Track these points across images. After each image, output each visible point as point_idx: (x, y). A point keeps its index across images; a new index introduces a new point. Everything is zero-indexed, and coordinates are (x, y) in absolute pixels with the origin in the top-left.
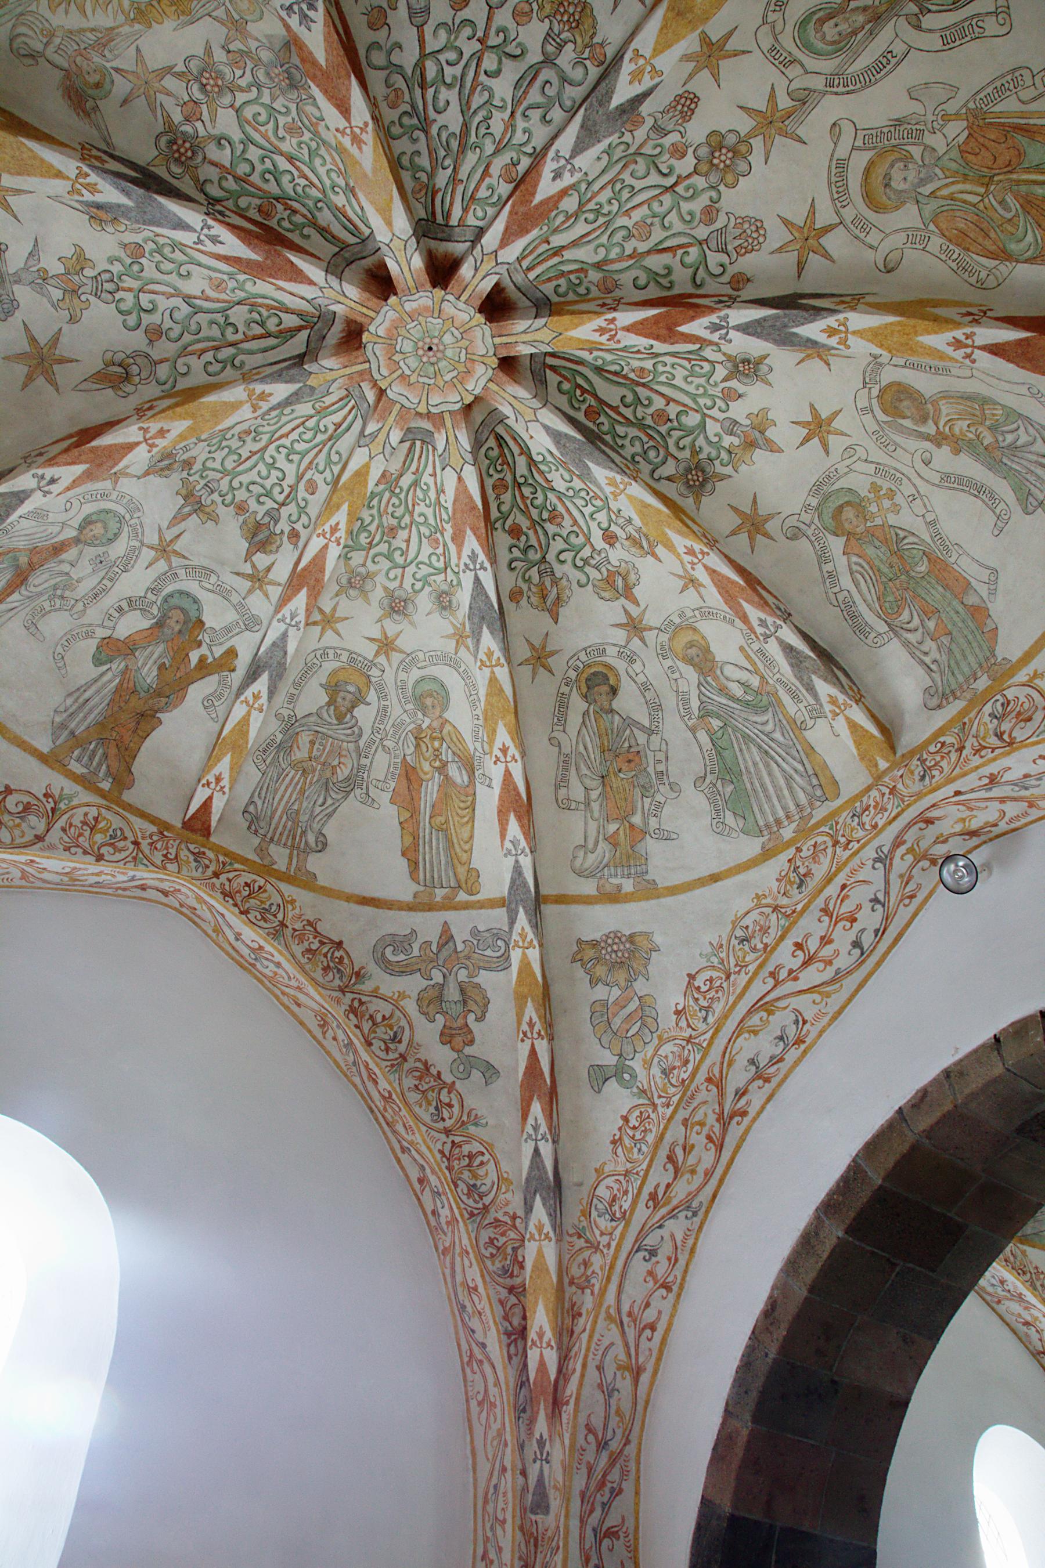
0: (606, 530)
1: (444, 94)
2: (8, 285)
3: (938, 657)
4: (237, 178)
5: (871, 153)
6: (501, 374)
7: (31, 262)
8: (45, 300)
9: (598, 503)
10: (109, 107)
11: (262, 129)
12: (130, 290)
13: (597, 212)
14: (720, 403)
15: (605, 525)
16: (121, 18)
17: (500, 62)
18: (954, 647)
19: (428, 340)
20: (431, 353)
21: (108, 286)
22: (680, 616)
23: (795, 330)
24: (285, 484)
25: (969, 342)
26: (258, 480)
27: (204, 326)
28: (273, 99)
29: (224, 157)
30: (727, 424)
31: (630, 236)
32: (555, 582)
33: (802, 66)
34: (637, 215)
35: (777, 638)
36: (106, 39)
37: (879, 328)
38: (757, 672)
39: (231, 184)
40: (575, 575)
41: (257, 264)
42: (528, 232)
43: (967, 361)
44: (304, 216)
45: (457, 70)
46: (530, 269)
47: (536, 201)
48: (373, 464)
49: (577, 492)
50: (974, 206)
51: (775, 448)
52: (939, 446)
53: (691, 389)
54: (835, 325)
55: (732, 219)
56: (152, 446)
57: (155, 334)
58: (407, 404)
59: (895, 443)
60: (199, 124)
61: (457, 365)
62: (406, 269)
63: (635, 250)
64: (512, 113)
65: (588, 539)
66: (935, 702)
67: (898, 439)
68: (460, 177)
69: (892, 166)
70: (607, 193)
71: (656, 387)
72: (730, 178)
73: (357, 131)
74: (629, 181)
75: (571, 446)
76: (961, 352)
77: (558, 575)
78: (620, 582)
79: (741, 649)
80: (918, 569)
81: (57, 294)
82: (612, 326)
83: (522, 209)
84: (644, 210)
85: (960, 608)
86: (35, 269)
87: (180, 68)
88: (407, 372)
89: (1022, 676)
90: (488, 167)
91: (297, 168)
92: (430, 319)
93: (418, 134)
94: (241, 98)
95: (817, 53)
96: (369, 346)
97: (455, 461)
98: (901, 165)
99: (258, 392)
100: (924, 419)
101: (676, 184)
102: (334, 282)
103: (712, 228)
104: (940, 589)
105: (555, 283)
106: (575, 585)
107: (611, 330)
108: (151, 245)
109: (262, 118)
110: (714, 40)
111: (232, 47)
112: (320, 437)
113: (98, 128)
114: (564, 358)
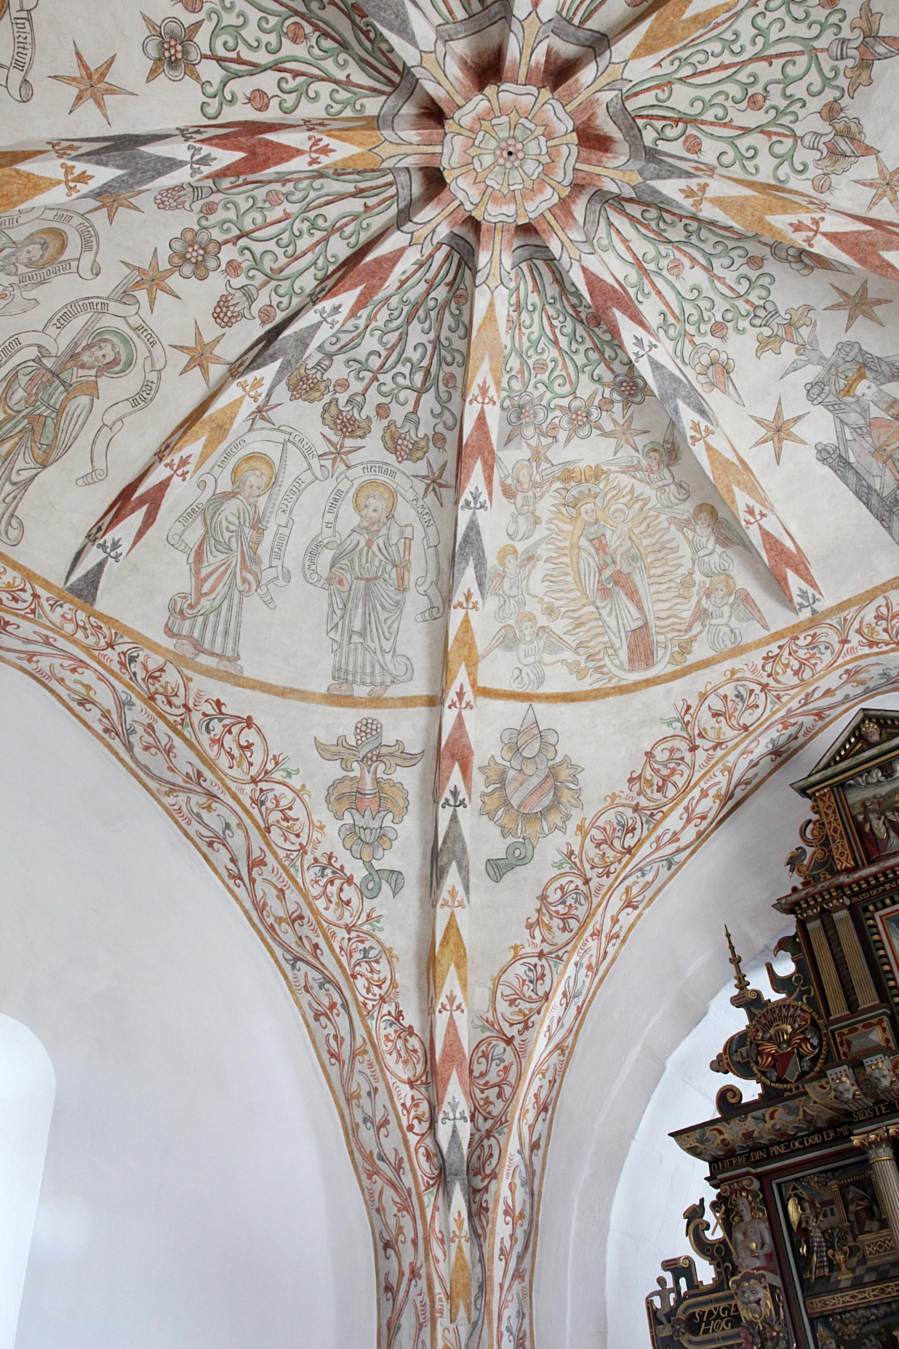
1: (415, 356)
2: (831, 361)
4: (602, 353)
5: (61, 259)
6: (446, 110)
7: (800, 363)
8: (817, 333)
10: (658, 436)
11: (564, 373)
12: (747, 301)
13: (314, 226)
16: (612, 476)
17: (367, 360)
19: (508, 165)
20: (511, 149)
21: (761, 313)
23: (120, 172)
24: (761, 8)
26: (788, 20)
27: (711, 243)
28: (541, 397)
29: (601, 370)
31: (287, 195)
33: (128, 324)
34: (277, 213)
36: (630, 469)
37: (35, 194)
39: (608, 352)
41: (619, 307)
44: (568, 300)
45: (399, 368)
46: (390, 184)
47: (361, 287)
48: (628, 53)
55: (187, 206)
56: (816, 222)
57: (755, 262)
58: (558, 106)
60: (607, 395)
61: (489, 129)
62: (497, 253)
63: (284, 185)
64: (367, 327)
68: (426, 285)
69: (42, 256)
70: (304, 243)
71: (283, 9)
72: (189, 236)
73: (480, 399)
74: (279, 252)
75: (388, 14)
81: (805, 331)
82: (314, 155)
83: (375, 282)
84: (271, 216)
86: (803, 357)
87: (596, 432)
88: (542, 139)
90: (400, 287)
91: (554, 334)
92: (497, 187)
93: (446, 343)
94: (564, 402)
95: (116, 333)
96: (567, 182)
97: (532, 27)
99: (691, 200)
101: (239, 238)
102: (565, 261)
107: (316, 151)
108: (704, 328)
109: (560, 381)
110: (198, 368)
111: (550, 440)
112: (684, 54)
113: (672, 433)
114: (380, 73)
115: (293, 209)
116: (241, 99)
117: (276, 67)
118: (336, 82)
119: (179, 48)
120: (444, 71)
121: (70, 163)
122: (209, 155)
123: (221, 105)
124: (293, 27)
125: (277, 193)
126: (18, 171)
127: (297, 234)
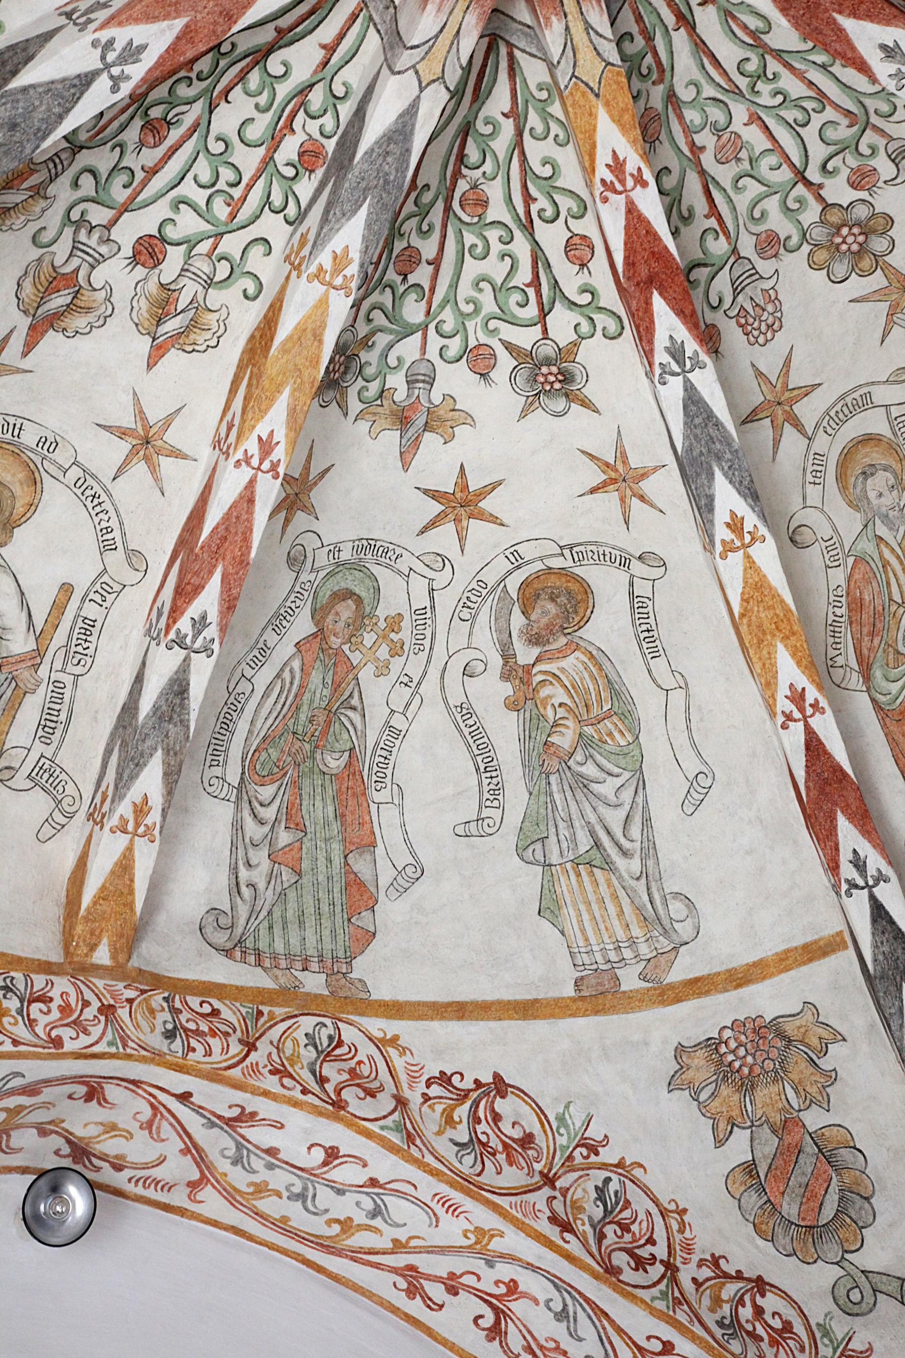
0: (163, 240)
3: (261, 886)
5: (889, 434)
9: (221, 210)
13: (762, 74)
14: (455, 346)
15: (171, 233)
18: (292, 895)
22: (43, 441)
23: (718, 474)
25: (809, 711)
30: (423, 368)
31: (718, 131)
32: (39, 192)
34: (754, 136)
35: (187, 659)
37: (770, 588)
38: (42, 638)
40: (54, 218)
42: (784, 11)
43: (780, 719)
49: (223, 158)
50: (891, 599)
51: (408, 457)
52: (506, 676)
53: (465, 290)
54: (748, 527)
55: (771, 283)
59: (474, 617)
63: (702, 149)
65: (125, 208)
66: (221, 938)
67: (484, 617)
70: (796, 88)
71: (450, 228)
72: (821, 256)
74: (817, 120)
76: (790, 707)
77: (51, 190)
78: (59, 301)
79: (67, 589)
80: (328, 759)
82: (630, 183)
85: (337, 860)
89: (376, 1026)
98: (892, 481)
100: (535, 639)
101: (808, 184)
103: (754, 258)
104: (331, 809)
105: (635, 29)
106: (33, 227)
107: (622, 182)
114: (484, 66)
115: (740, 112)
116: (584, 278)
117: (528, 227)
118: (519, 134)
119: (544, 370)
120: (437, 37)
121: (719, 548)
122: (667, 349)
123: (600, 309)
124: (467, 209)
125: (719, 149)
126: (742, 615)
127: (780, 98)
